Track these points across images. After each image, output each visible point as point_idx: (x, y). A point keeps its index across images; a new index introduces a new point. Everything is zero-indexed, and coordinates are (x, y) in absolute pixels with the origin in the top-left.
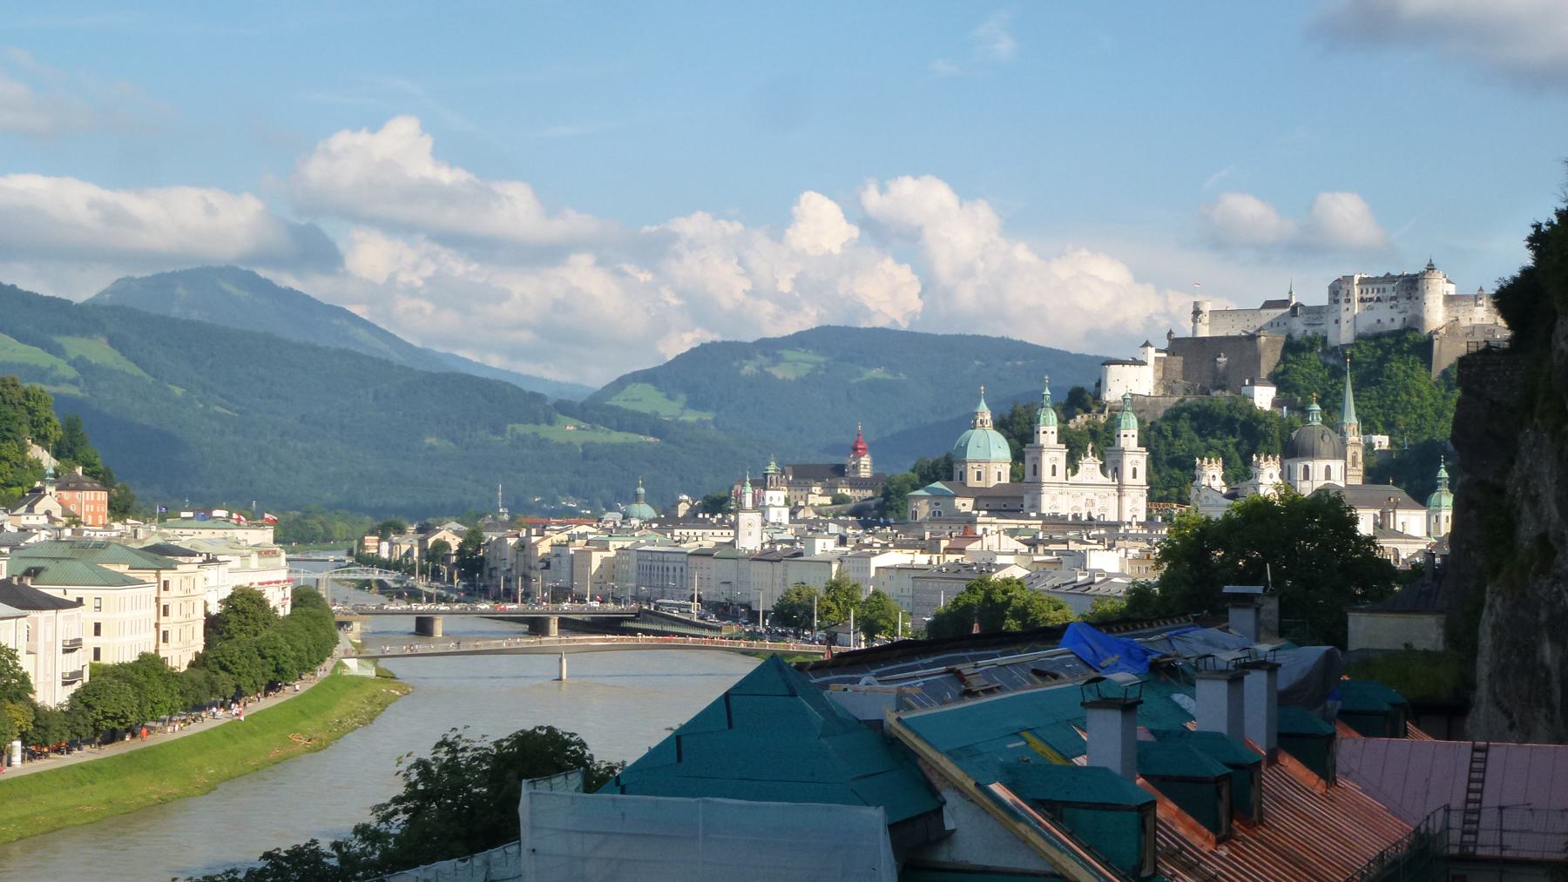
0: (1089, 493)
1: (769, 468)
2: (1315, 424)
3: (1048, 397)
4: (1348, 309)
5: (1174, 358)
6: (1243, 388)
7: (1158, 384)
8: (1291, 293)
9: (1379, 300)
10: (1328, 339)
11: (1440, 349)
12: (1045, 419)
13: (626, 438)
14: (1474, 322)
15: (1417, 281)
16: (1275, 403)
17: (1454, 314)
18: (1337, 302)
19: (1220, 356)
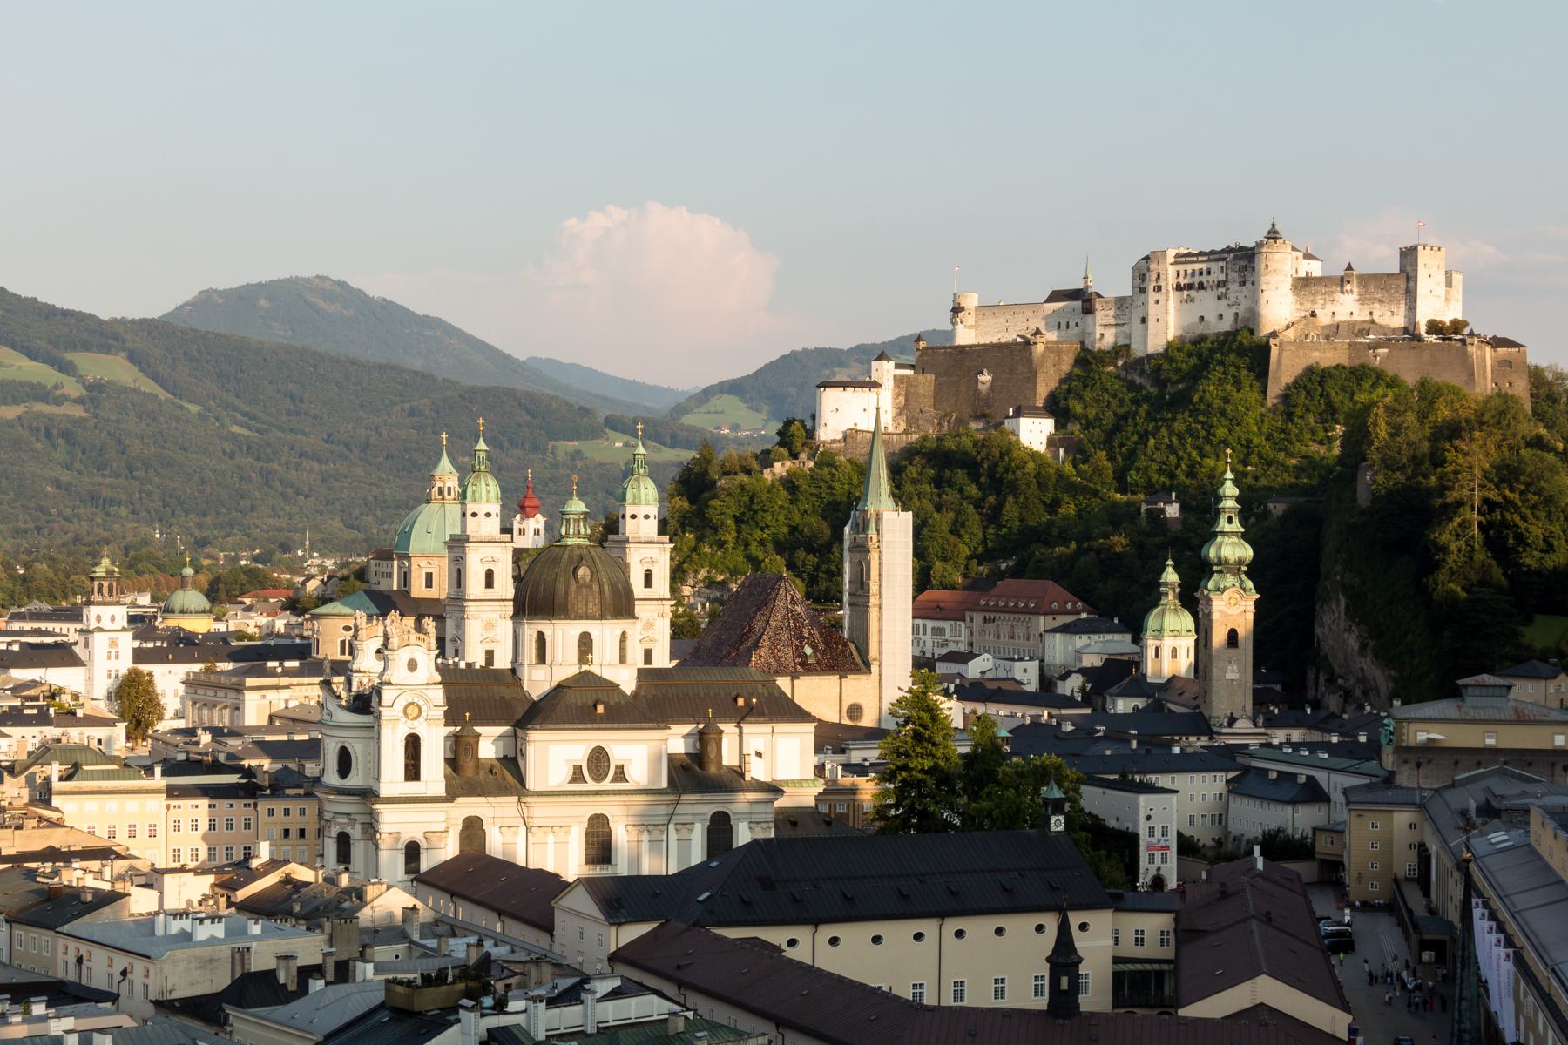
1: (97, 569)
2: (570, 542)
3: (482, 454)
4: (1157, 302)
5: (921, 377)
6: (1006, 421)
7: (900, 414)
9: (1201, 286)
10: (1133, 346)
11: (1279, 361)
12: (474, 492)
13: (678, 455)
16: (1051, 442)
17: (1309, 307)
18: (1143, 290)
19: (982, 373)
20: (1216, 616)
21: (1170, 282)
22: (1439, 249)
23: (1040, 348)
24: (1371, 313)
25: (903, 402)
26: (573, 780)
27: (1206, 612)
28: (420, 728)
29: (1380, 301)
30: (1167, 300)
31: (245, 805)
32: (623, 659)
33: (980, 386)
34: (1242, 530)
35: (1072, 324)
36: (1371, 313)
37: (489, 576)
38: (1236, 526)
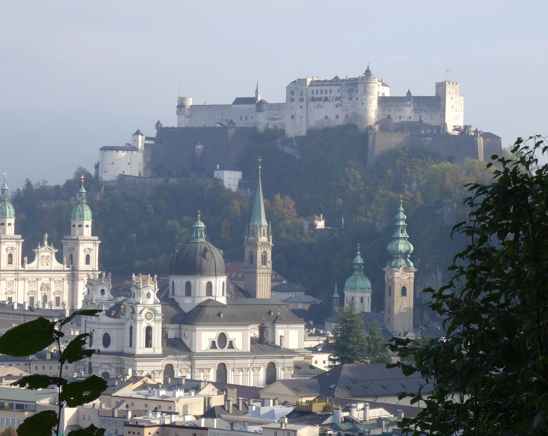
0: (45, 279)
4: (301, 107)
6: (215, 172)
8: (257, 91)
9: (326, 99)
14: (403, 120)
15: (356, 84)
17: (387, 113)
19: (197, 144)
20: (396, 280)
21: (308, 96)
22: (456, 83)
23: (232, 131)
24: (420, 118)
25: (150, 159)
26: (212, 348)
27: (390, 278)
28: (152, 324)
29: (426, 111)
30: (307, 106)
31: (25, 365)
32: (223, 295)
33: (196, 151)
34: (408, 236)
35: (249, 118)
36: (420, 118)
37: (88, 258)
38: (405, 235)
